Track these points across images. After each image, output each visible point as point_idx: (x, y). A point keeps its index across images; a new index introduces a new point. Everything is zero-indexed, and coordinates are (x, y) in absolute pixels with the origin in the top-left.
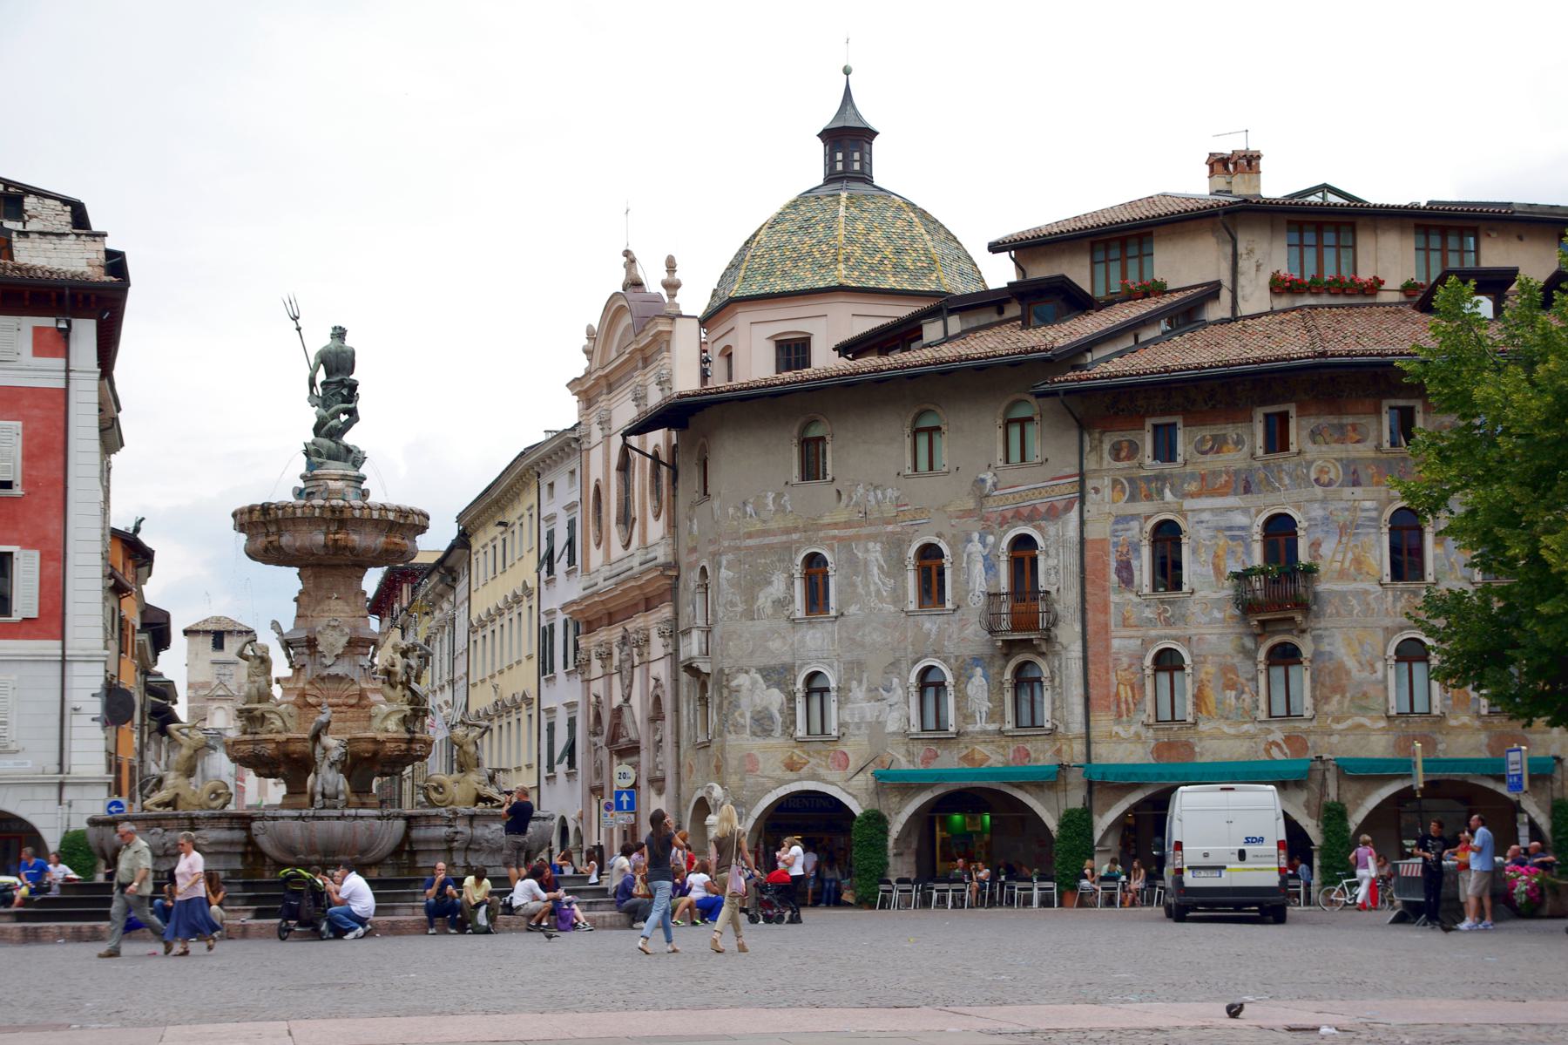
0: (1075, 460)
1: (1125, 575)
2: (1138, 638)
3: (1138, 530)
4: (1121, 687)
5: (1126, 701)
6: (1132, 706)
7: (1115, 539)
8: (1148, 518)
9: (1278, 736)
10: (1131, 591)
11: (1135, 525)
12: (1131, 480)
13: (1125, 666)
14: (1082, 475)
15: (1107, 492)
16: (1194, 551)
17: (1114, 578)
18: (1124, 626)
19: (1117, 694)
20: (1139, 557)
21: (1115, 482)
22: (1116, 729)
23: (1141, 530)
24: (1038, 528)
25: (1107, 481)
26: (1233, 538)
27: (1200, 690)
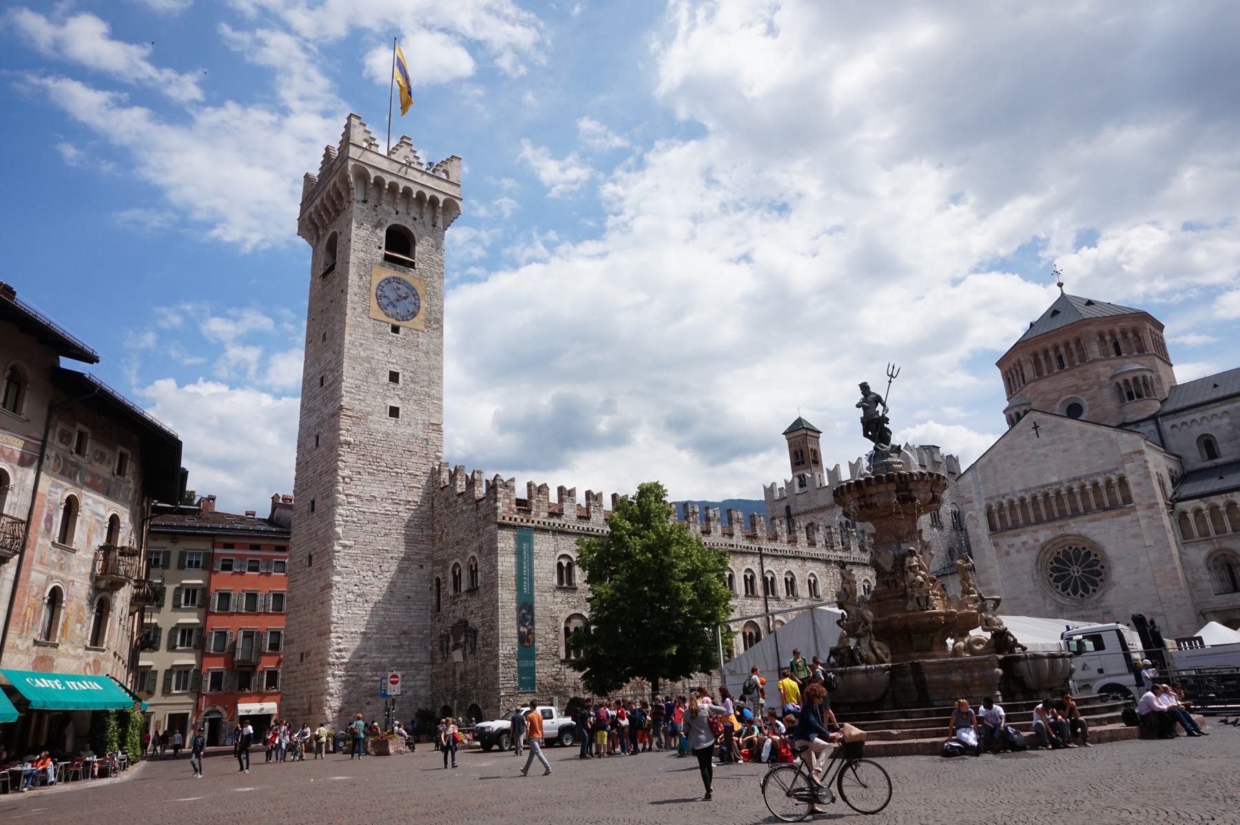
0: (42, 429)
1: (48, 525)
2: (45, 574)
3: (60, 496)
4: (29, 609)
5: (29, 623)
6: (31, 625)
7: (49, 497)
8: (67, 490)
9: (90, 660)
10: (49, 538)
11: (60, 491)
12: (65, 460)
13: (34, 593)
14: (44, 441)
15: (52, 461)
16: (82, 522)
17: (43, 525)
18: (40, 563)
19: (25, 614)
20: (57, 515)
21: (57, 457)
22: (18, 642)
23: (62, 496)
24: (15, 471)
25: (53, 454)
26: (98, 521)
27: (66, 621)
